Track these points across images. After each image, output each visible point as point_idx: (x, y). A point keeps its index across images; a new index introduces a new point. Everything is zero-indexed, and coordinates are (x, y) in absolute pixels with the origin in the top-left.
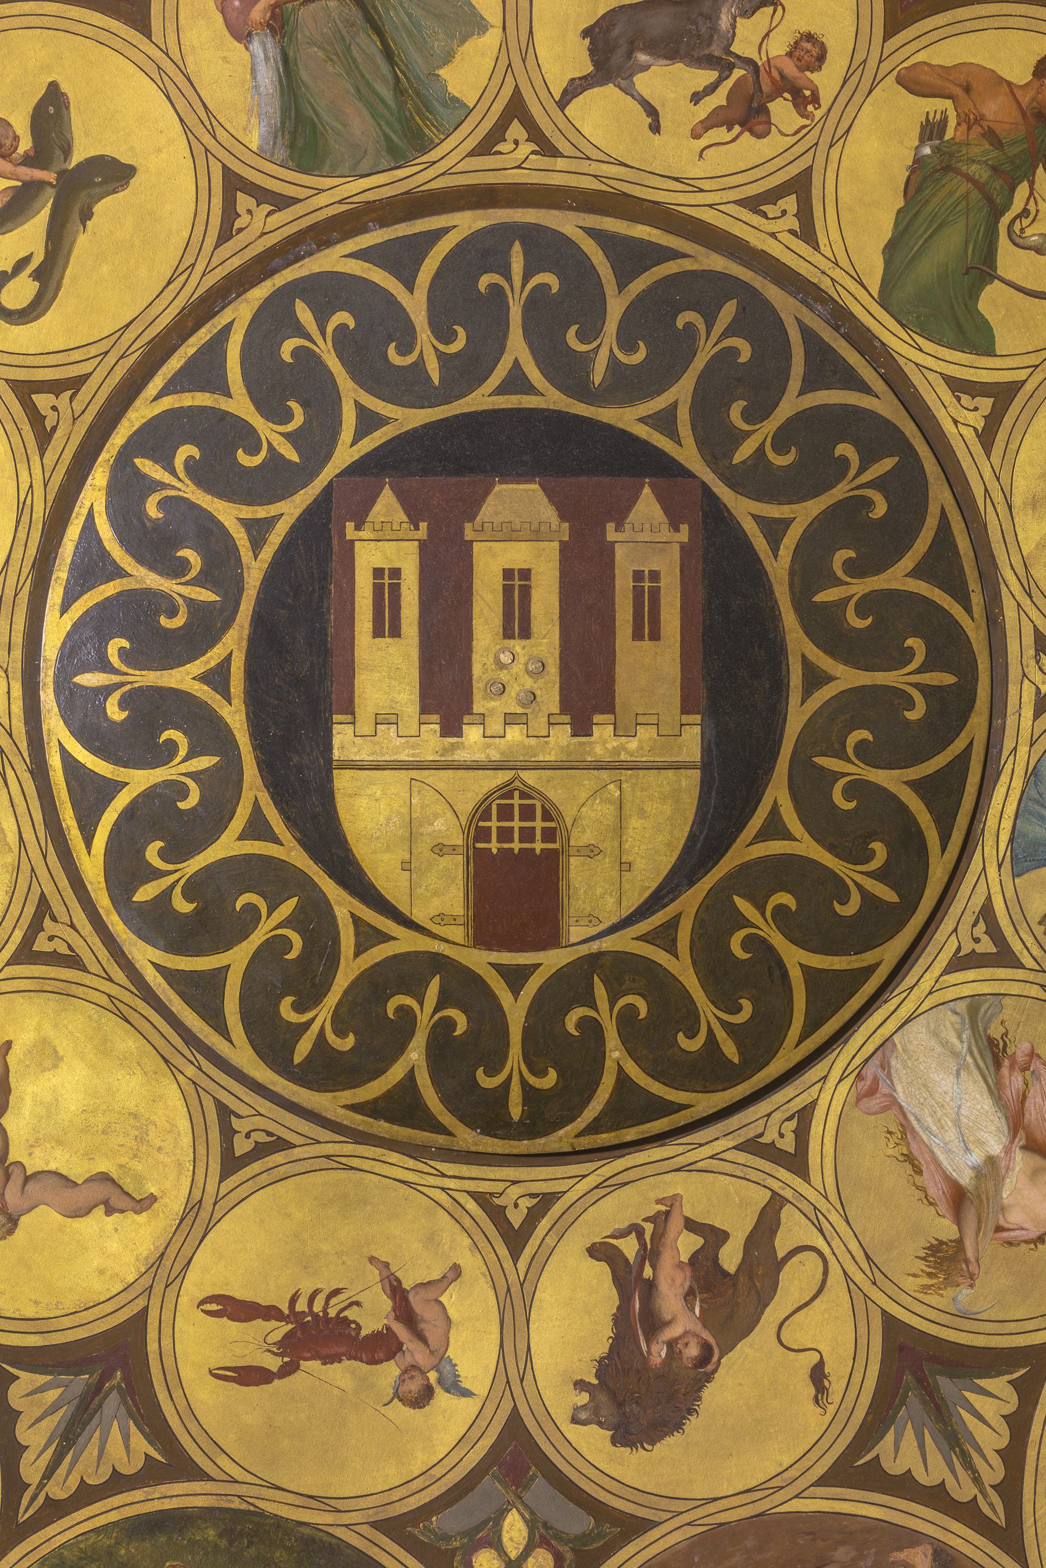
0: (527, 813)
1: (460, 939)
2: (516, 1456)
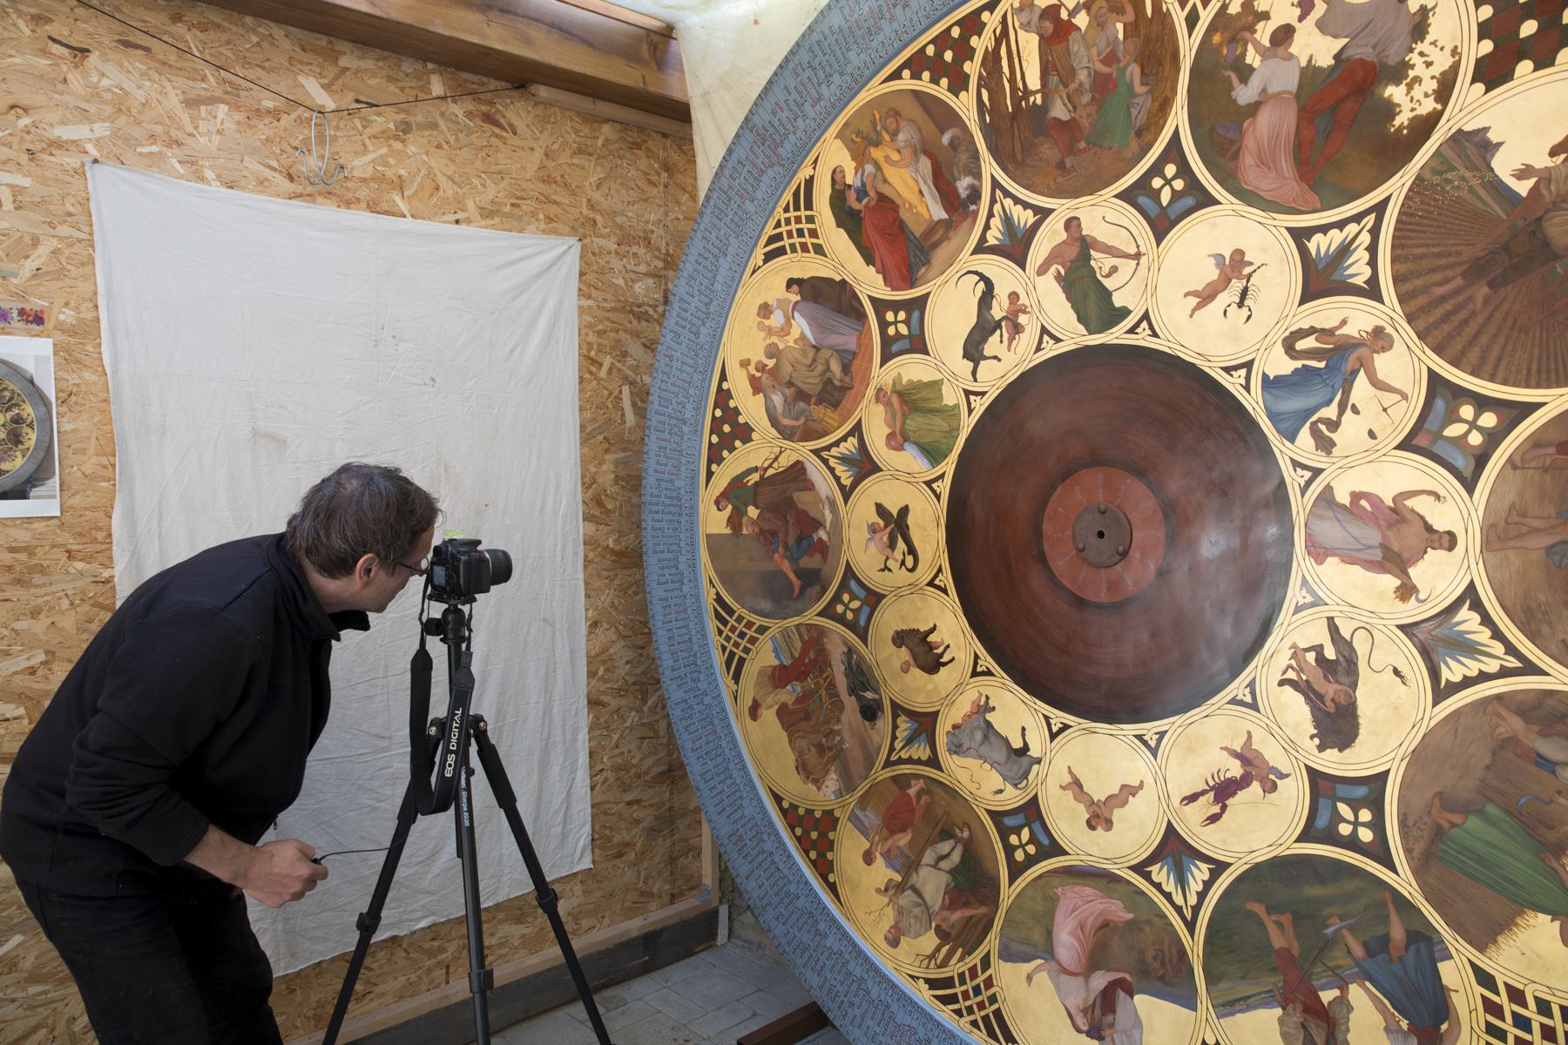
2: (1319, 782)
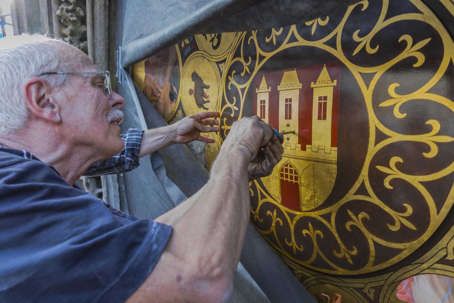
0: (291, 171)
1: (279, 202)
